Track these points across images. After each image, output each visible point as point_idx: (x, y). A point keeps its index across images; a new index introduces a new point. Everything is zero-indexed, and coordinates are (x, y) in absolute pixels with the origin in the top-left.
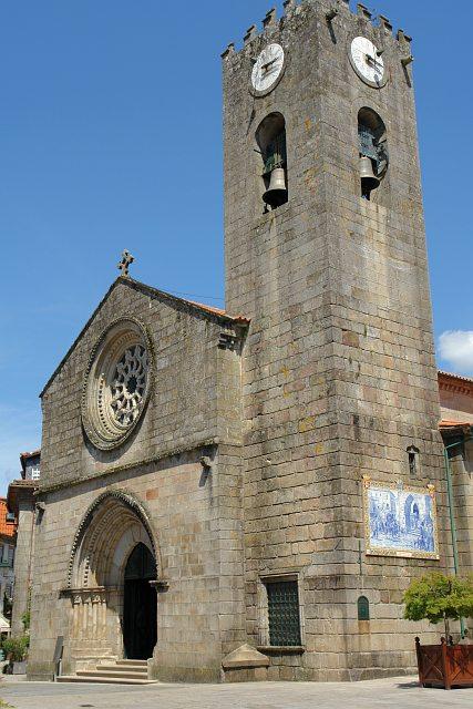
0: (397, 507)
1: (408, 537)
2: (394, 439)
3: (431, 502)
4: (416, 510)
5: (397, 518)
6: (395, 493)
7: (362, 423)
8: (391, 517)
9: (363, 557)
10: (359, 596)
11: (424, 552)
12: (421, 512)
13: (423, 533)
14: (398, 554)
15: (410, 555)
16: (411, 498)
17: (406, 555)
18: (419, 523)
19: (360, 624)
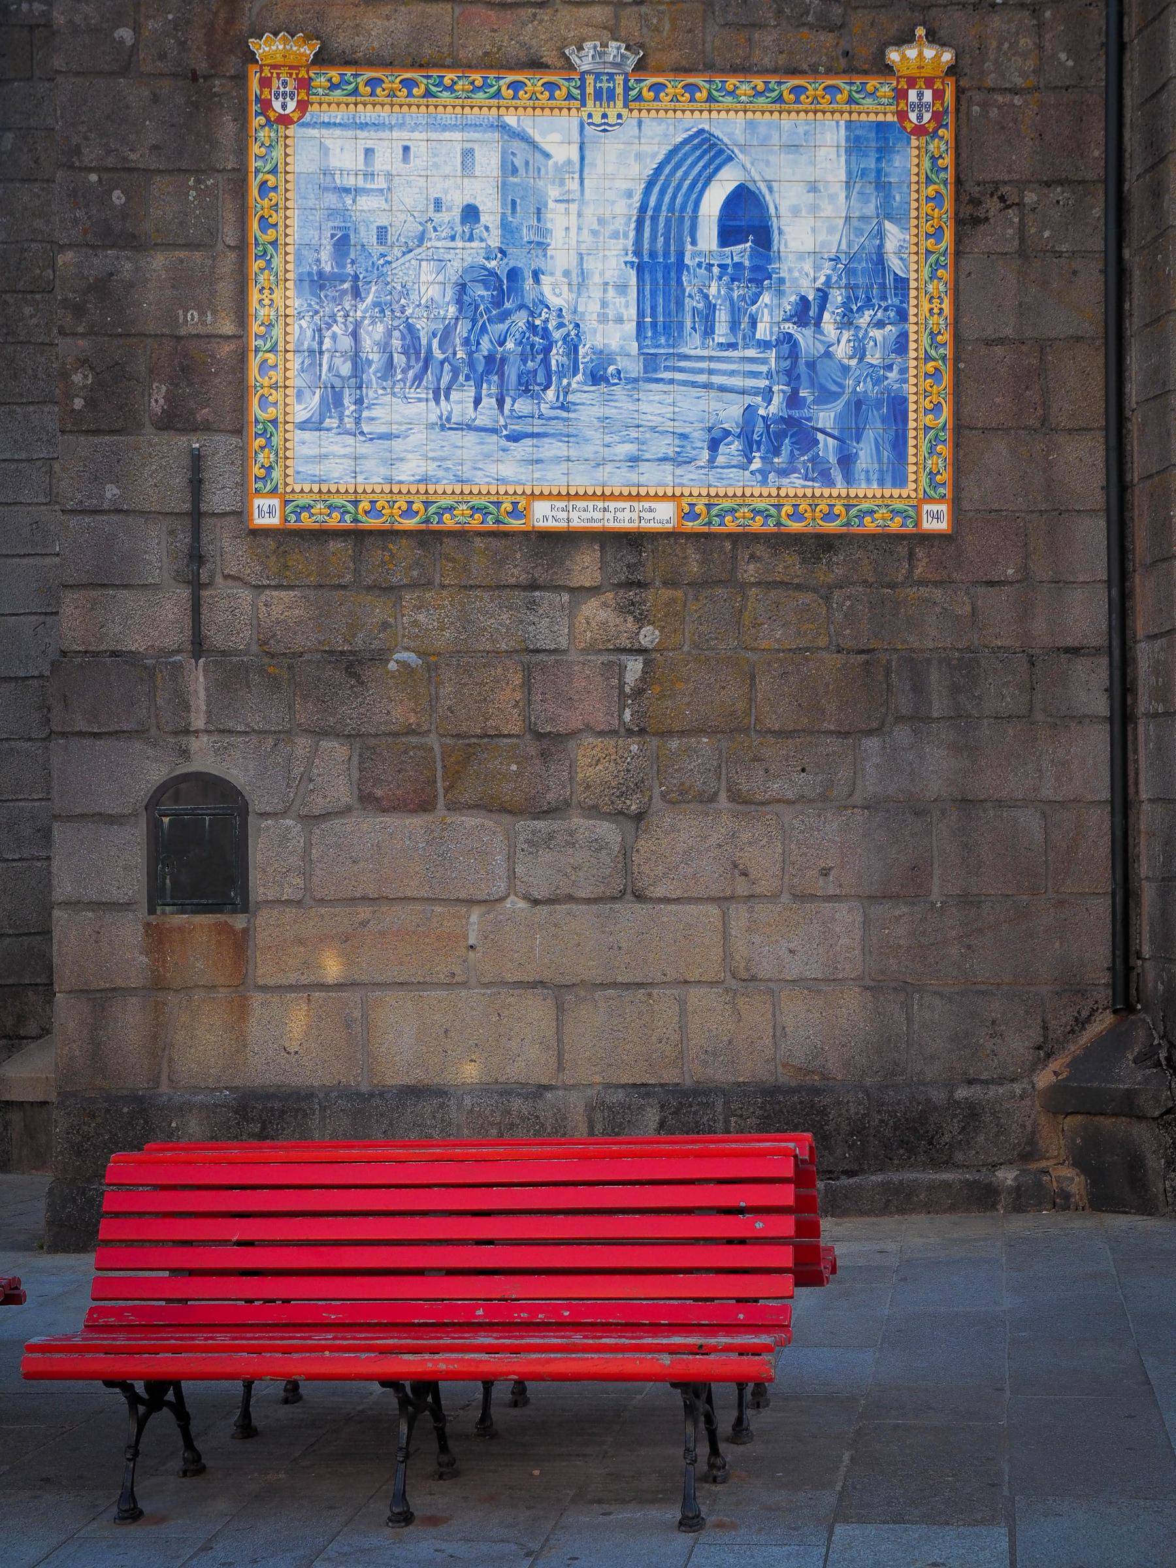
0: (558, 220)
1: (655, 405)
4: (747, 219)
5: (555, 292)
6: (556, 134)
9: (229, 552)
11: (794, 485)
12: (808, 237)
15: (662, 516)
17: (623, 517)
19: (156, 938)
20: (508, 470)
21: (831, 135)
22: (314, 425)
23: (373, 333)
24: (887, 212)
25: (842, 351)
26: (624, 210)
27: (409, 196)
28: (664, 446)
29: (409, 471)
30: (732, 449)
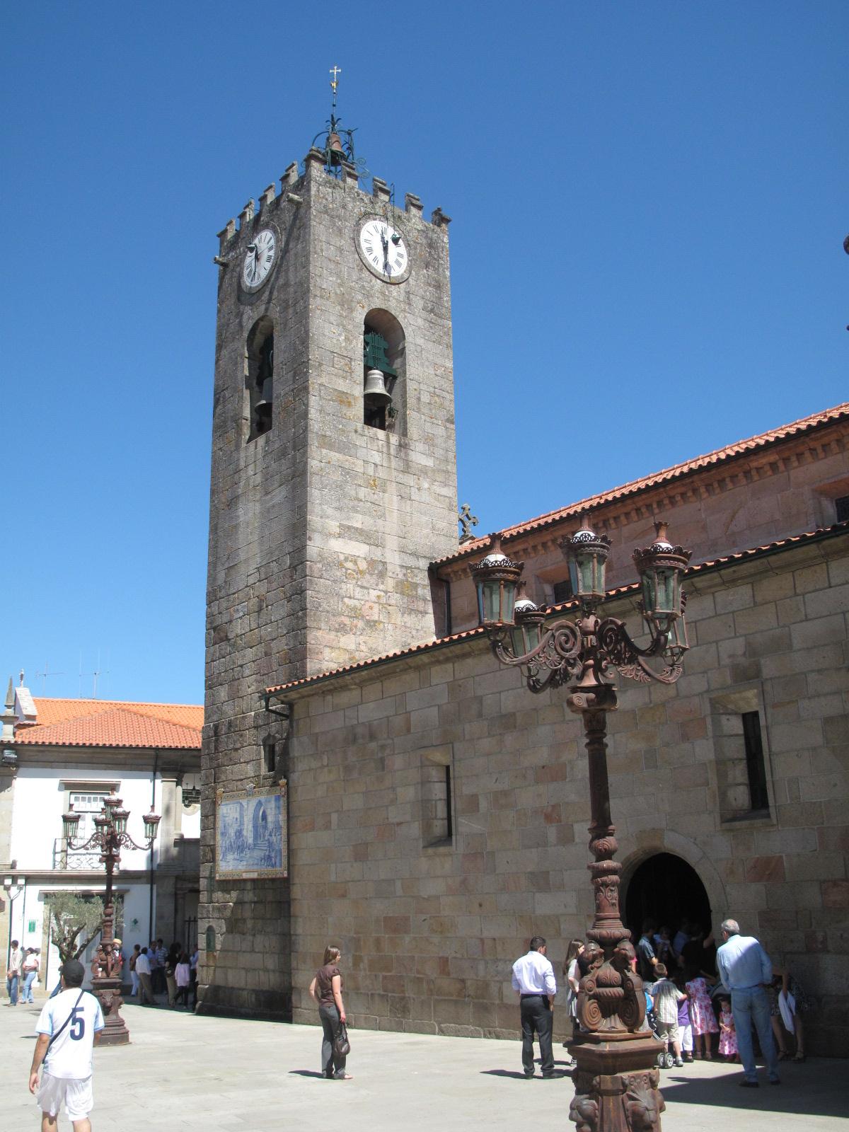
0: (245, 819)
2: (249, 735)
3: (282, 802)
4: (264, 817)
5: (245, 833)
7: (224, 729)
8: (239, 833)
10: (207, 925)
11: (270, 868)
12: (270, 819)
13: (270, 844)
14: (245, 876)
15: (255, 876)
16: (260, 803)
18: (267, 833)
19: (207, 956)
20: (240, 867)
21: (273, 799)
22: (221, 860)
23: (228, 842)
24: (280, 813)
25: (275, 841)
26: (251, 816)
27: (231, 817)
28: (256, 862)
29: (231, 868)
30: (263, 861)
